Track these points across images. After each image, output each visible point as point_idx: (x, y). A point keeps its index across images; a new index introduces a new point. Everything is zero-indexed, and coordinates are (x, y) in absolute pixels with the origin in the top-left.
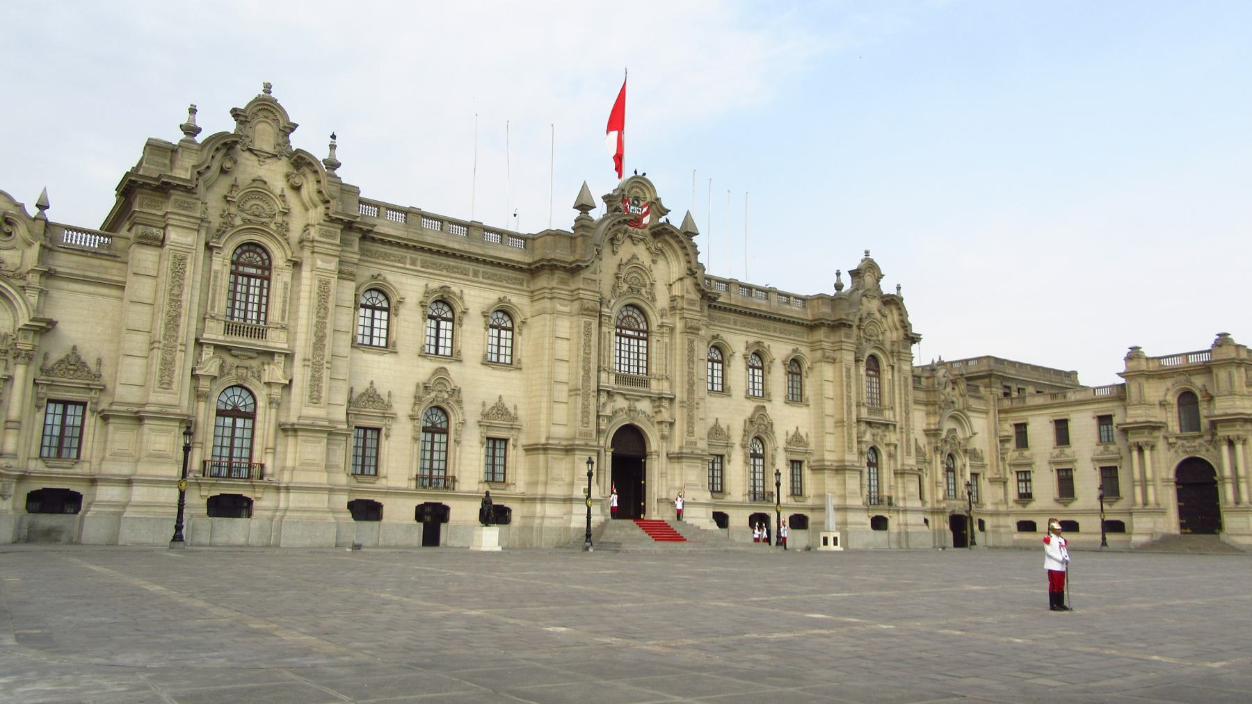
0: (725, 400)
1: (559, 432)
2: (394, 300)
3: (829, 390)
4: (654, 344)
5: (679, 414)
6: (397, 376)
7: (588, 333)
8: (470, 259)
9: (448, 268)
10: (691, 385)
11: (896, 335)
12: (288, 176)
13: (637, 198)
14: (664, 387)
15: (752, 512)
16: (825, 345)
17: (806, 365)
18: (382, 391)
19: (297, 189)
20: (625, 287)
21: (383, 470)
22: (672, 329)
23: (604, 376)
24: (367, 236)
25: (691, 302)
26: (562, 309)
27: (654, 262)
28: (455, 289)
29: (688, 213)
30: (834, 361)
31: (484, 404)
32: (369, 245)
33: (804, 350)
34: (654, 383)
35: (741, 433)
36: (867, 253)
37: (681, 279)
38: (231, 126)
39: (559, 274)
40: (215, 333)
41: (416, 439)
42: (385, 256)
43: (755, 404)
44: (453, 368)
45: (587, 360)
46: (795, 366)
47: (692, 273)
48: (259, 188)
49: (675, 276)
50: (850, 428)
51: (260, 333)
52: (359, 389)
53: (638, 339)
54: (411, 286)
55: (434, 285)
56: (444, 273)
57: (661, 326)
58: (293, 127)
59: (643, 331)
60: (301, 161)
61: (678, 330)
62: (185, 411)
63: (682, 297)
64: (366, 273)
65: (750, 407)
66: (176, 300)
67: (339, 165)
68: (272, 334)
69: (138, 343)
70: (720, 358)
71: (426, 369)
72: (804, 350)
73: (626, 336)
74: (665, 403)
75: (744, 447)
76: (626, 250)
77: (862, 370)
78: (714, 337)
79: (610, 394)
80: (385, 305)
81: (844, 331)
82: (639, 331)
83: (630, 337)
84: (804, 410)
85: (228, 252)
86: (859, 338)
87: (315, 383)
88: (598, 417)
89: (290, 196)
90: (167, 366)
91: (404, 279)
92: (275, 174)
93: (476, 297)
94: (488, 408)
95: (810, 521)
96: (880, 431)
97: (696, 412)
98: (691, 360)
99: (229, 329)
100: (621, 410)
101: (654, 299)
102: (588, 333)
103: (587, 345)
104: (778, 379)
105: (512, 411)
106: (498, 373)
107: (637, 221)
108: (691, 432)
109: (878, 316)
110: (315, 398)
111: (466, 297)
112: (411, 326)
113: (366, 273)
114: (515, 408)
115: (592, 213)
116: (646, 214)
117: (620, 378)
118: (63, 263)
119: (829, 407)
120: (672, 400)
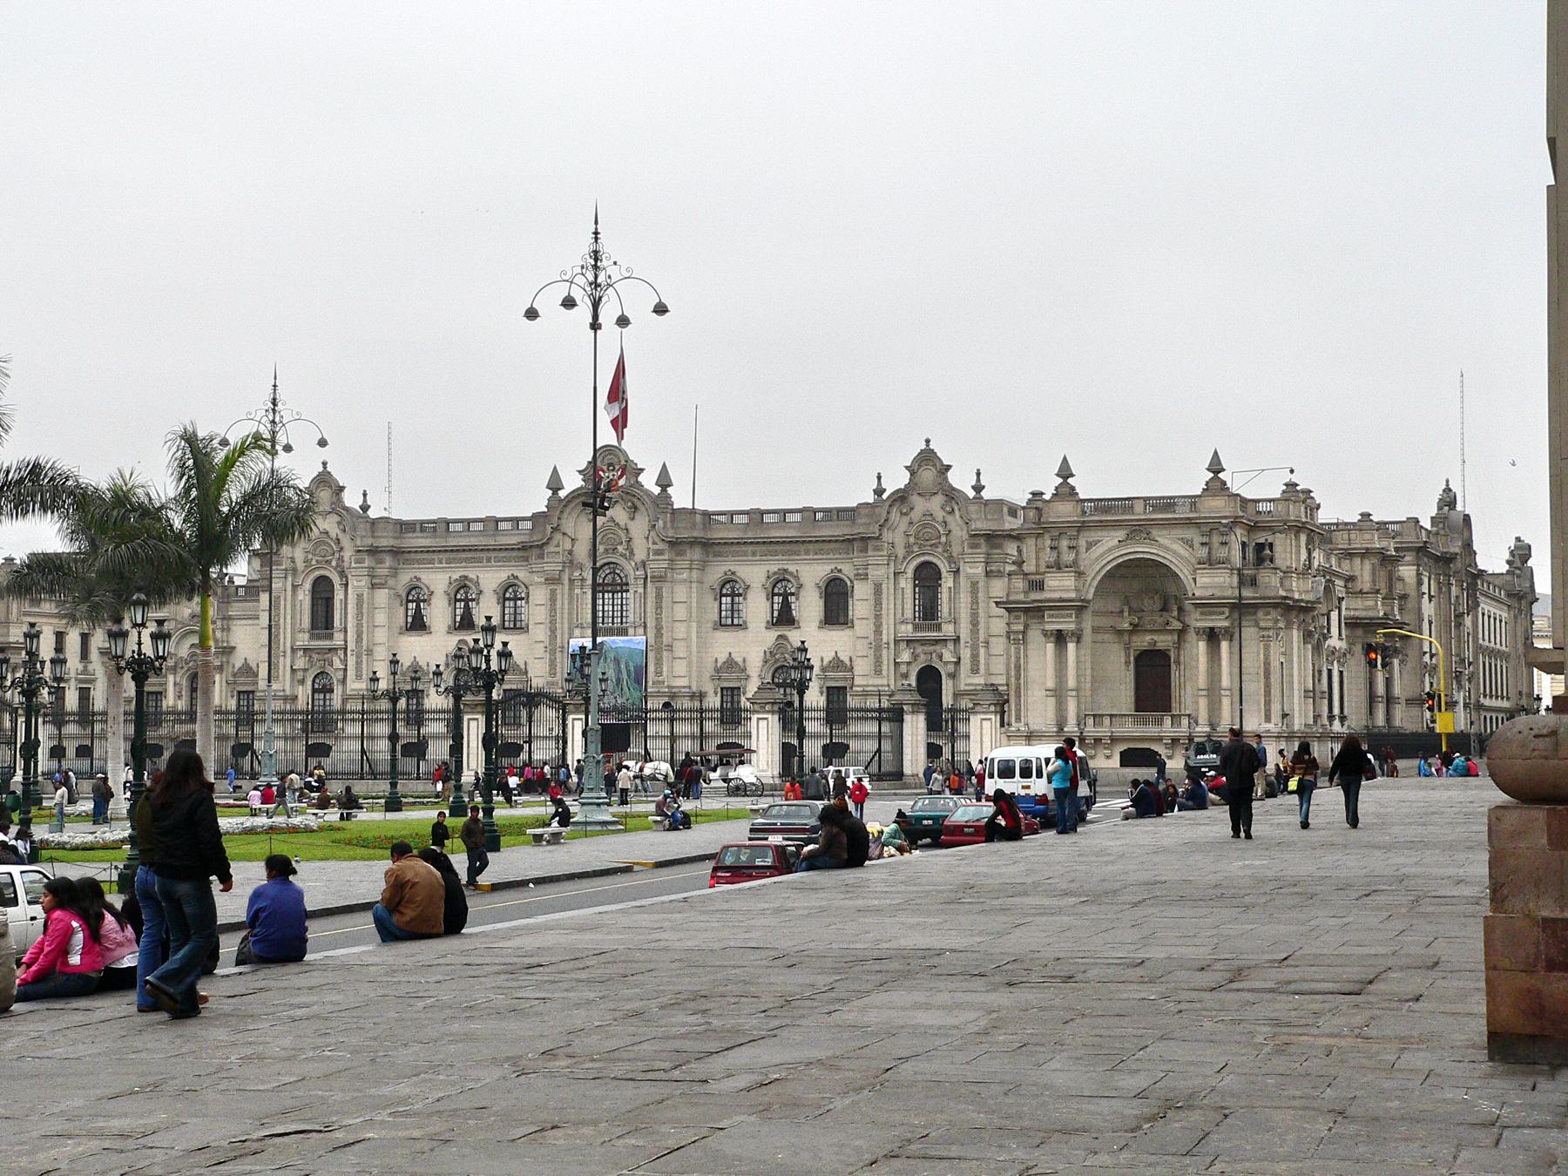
0: (741, 633)
7: (553, 599)
9: (466, 560)
10: (659, 629)
11: (965, 536)
13: (610, 465)
24: (396, 552)
25: (658, 552)
28: (472, 576)
32: (402, 557)
36: (928, 441)
39: (535, 552)
40: (303, 640)
42: (419, 562)
45: (553, 622)
50: (878, 648)
51: (330, 637)
54: (438, 580)
55: (456, 576)
58: (342, 489)
64: (405, 578)
65: (772, 635)
68: (336, 635)
72: (847, 570)
77: (906, 584)
81: (871, 544)
82: (621, 585)
84: (848, 632)
85: (308, 586)
86: (908, 546)
91: (432, 576)
96: (938, 647)
98: (659, 607)
99: (312, 637)
101: (632, 553)
103: (553, 609)
104: (810, 607)
108: (659, 673)
109: (940, 515)
110: (359, 677)
113: (405, 578)
118: (235, 609)
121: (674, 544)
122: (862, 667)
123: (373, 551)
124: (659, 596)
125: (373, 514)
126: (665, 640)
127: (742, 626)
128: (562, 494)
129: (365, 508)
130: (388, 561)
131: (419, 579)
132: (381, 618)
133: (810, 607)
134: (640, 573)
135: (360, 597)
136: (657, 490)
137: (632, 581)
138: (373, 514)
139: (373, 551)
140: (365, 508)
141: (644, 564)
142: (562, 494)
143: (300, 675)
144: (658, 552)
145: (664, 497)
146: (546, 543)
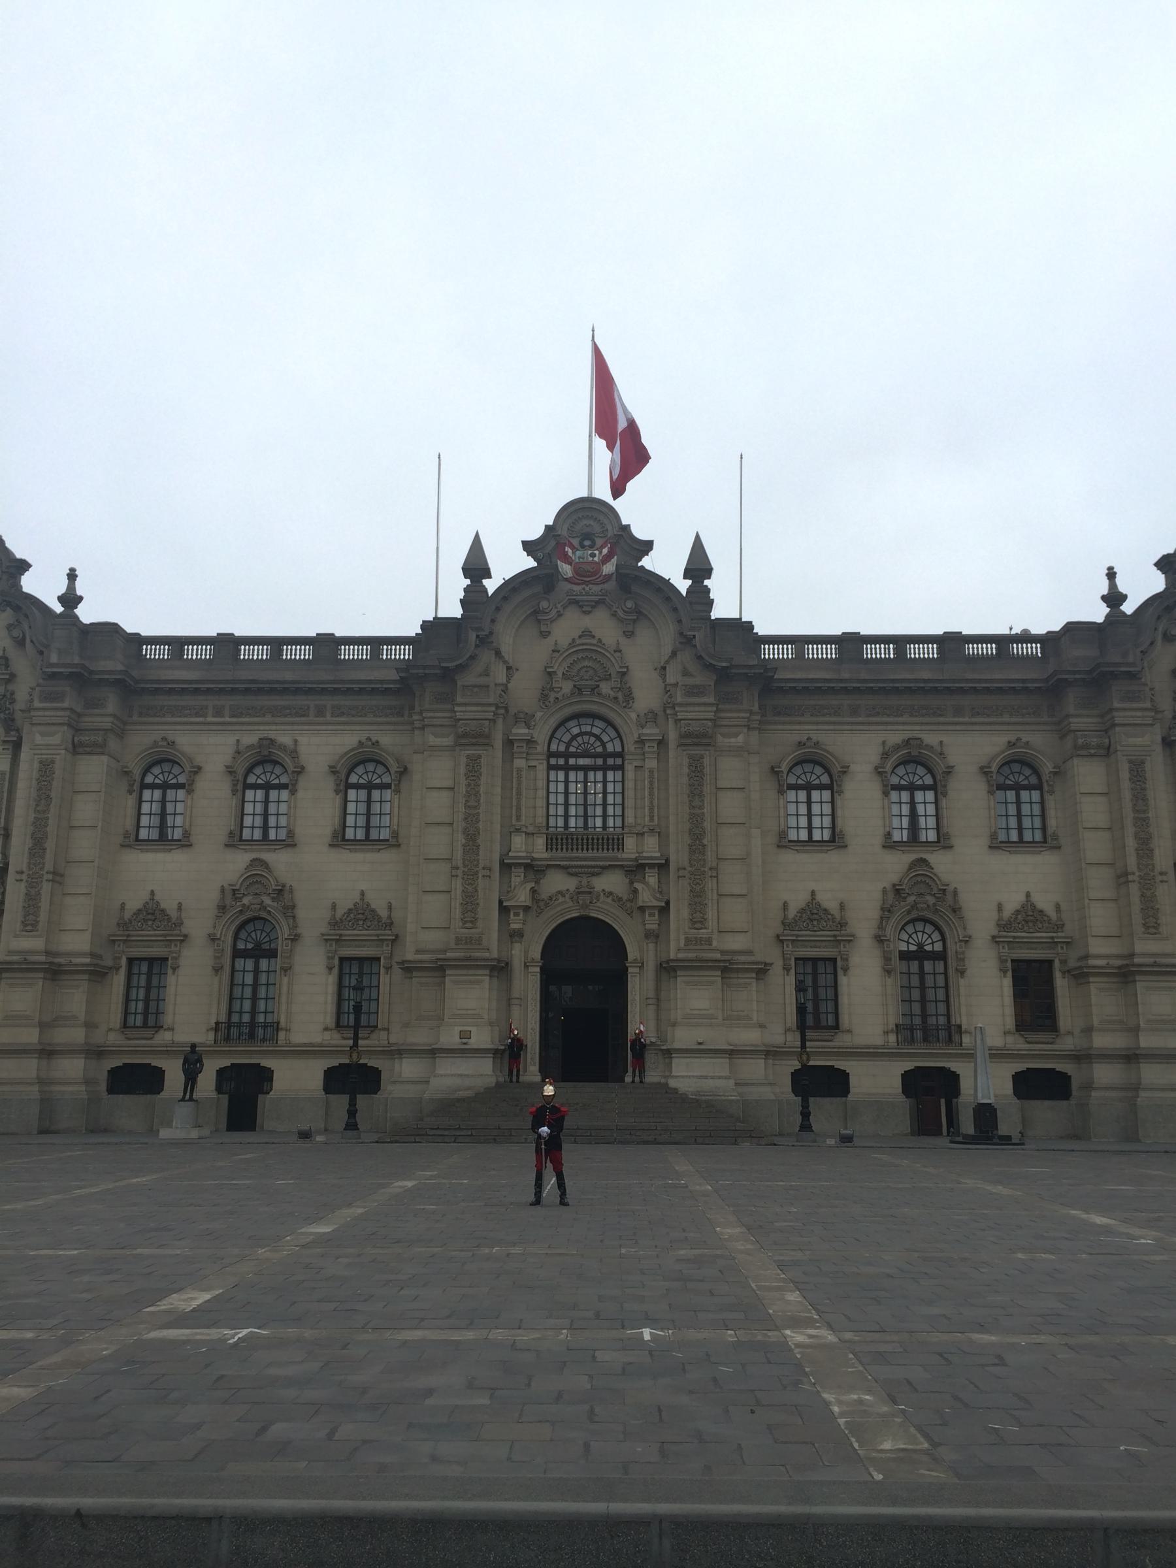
0: (833, 857)
1: (434, 939)
2: (188, 768)
3: (1094, 812)
4: (630, 773)
6: (190, 879)
7: (473, 770)
8: (310, 692)
10: (697, 836)
12: (10, 627)
13: (587, 536)
14: (650, 848)
15: (909, 1065)
16: (1076, 723)
17: (1047, 767)
18: (169, 905)
19: (20, 643)
20: (567, 687)
21: (168, 1020)
22: (662, 743)
23: (518, 841)
25: (693, 691)
26: (438, 741)
27: (629, 634)
28: (285, 739)
29: (698, 537)
30: (1107, 752)
31: (334, 907)
33: (1039, 741)
34: (630, 843)
35: (875, 914)
37: (674, 654)
41: (217, 970)
43: (913, 857)
44: (280, 861)
45: (472, 818)
46: (1015, 775)
47: (687, 641)
49: (667, 650)
52: (134, 904)
53: (605, 769)
56: (268, 718)
57: (641, 742)
59: (614, 755)
61: (672, 745)
62: (495, 955)
63: (676, 685)
64: (142, 740)
65: (896, 865)
67: (81, 599)
70: (825, 779)
71: (237, 863)
72: (1039, 741)
73: (577, 768)
74: (652, 879)
75: (880, 939)
76: (567, 628)
78: (801, 744)
79: (534, 869)
80: (928, 780)
82: (605, 755)
83: (585, 769)
87: (31, 901)
88: (504, 910)
89: (13, 653)
93: (320, 746)
94: (340, 913)
95: (1075, 1084)
97: (710, 884)
98: (695, 792)
100: (560, 893)
101: (629, 697)
102: (473, 770)
103: (473, 792)
104: (970, 804)
105: (383, 913)
106: (359, 856)
107: (585, 574)
108: (697, 920)
110: (29, 925)
111: (302, 750)
112: (209, 804)
113: (142, 740)
114: (390, 907)
115: (485, 582)
116: (606, 559)
117: (553, 841)
119: (1096, 847)
121: (724, 675)
122: (1100, 918)
123: (82, 680)
124: (696, 770)
125: (87, 614)
126: (710, 856)
127: (836, 840)
128: (491, 585)
129: (71, 599)
130: (112, 704)
131: (172, 744)
132: (86, 810)
134: (651, 731)
135: (46, 769)
136: (683, 585)
137: (630, 747)
138: (87, 614)
139: (82, 680)
140: (71, 599)
141: (651, 717)
142: (491, 585)
144: (693, 691)
145: (701, 597)
146: (462, 668)
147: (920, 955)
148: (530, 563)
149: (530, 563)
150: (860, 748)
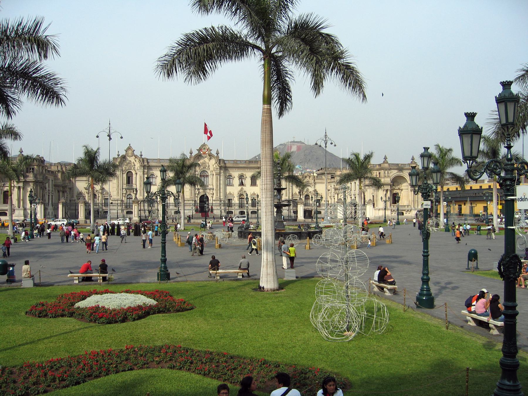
5: (214, 192)
25: (217, 169)
38: (124, 153)
40: (125, 186)
48: (130, 162)
60: (136, 157)
66: (118, 183)
69: (115, 189)
90: (118, 192)
92: (132, 159)
104: (248, 181)
107: (205, 153)
120: (213, 189)
121: (221, 168)
125: (143, 157)
127: (233, 185)
128: (193, 155)
133: (248, 181)
135: (141, 177)
138: (143, 157)
140: (141, 155)
142: (193, 155)
143: (124, 195)
145: (218, 157)
147: (242, 198)
148: (197, 152)
149: (197, 152)
150: (235, 174)
